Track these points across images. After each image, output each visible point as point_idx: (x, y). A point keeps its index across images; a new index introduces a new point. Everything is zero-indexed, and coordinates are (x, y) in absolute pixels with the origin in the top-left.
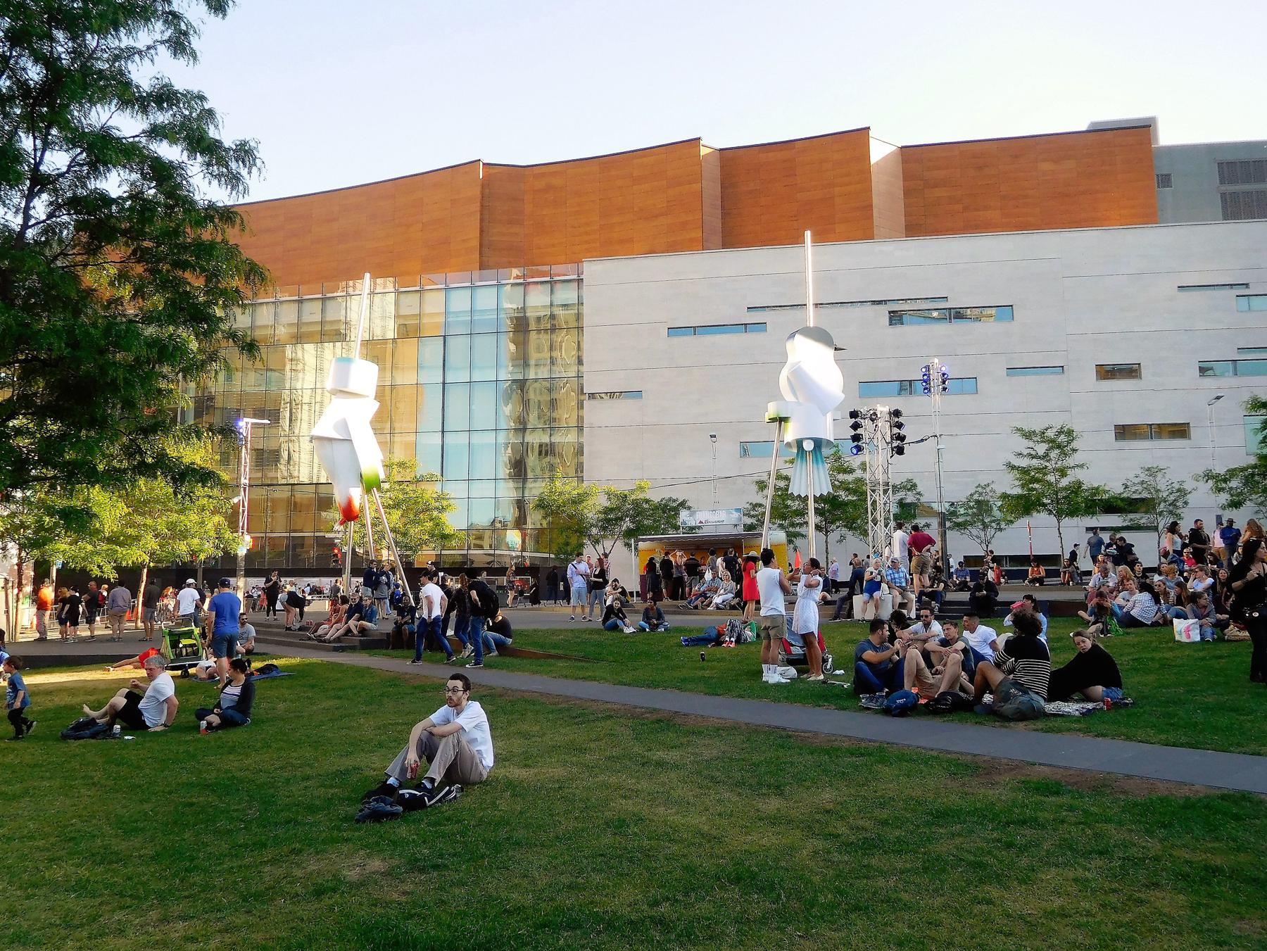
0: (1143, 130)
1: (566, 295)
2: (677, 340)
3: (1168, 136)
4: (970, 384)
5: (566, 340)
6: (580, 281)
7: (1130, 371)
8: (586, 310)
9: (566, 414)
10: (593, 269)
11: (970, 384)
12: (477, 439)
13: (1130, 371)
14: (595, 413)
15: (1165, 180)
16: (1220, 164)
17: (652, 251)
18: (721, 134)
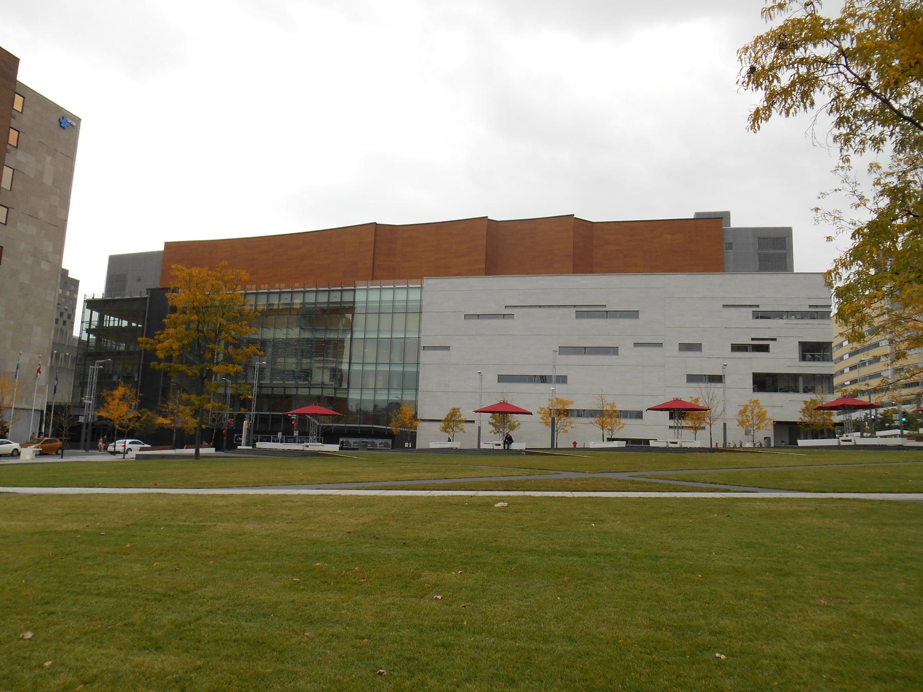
0: (721, 219)
1: (415, 295)
2: (468, 321)
3: (735, 223)
4: (614, 351)
5: (413, 318)
6: (421, 288)
7: (696, 347)
8: (424, 303)
9: (410, 358)
10: (429, 282)
11: (614, 351)
12: (367, 368)
13: (696, 347)
14: (425, 356)
15: (730, 246)
16: (759, 238)
17: (459, 274)
18: (499, 213)
